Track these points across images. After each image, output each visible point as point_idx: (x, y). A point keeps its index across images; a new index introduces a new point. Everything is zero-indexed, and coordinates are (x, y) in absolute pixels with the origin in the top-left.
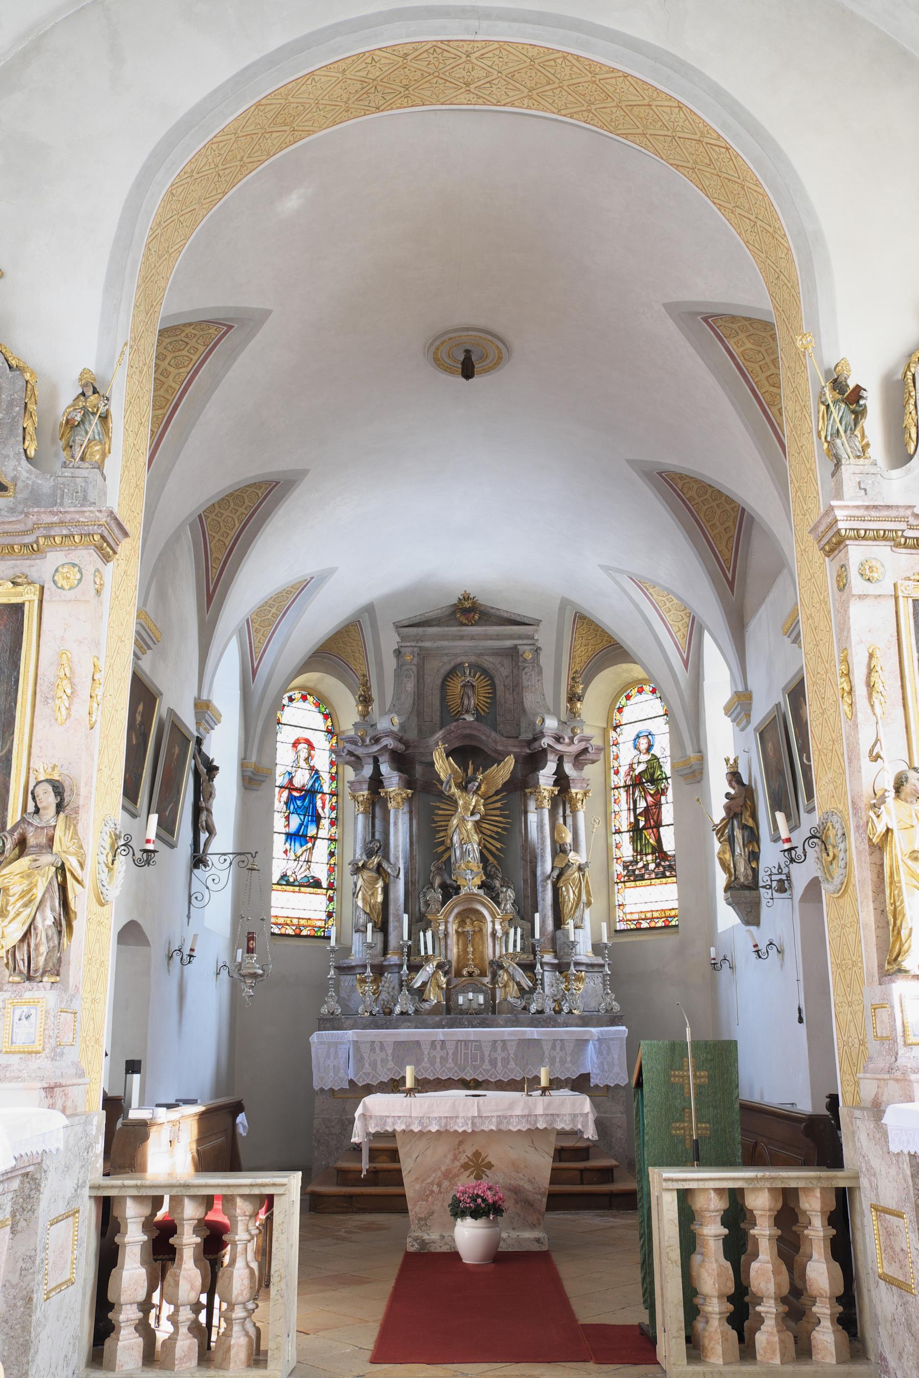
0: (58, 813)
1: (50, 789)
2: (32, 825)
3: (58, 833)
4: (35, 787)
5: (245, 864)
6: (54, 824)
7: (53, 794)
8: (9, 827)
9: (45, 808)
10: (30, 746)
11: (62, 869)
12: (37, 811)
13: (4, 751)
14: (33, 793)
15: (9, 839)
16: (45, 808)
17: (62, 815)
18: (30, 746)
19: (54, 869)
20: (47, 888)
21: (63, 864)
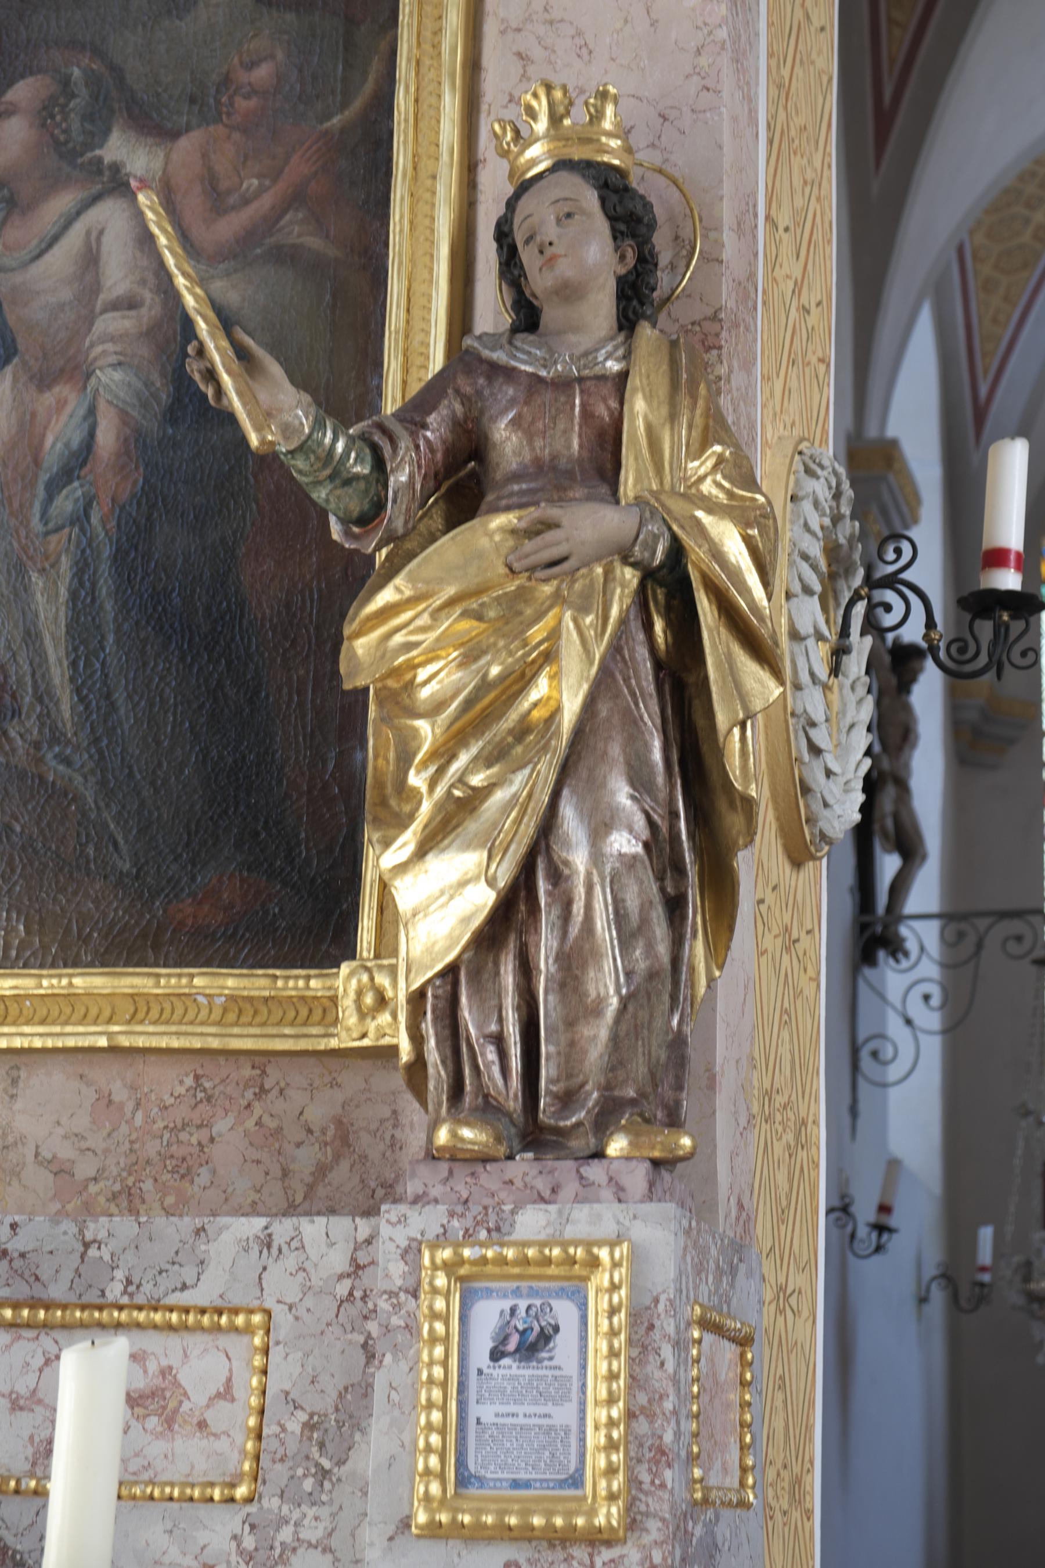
0: (627, 321)
1: (590, 198)
2: (509, 373)
3: (639, 409)
4: (511, 204)
5: (1027, 943)
6: (613, 366)
7: (602, 225)
8: (391, 404)
9: (570, 292)
10: (473, 66)
11: (671, 585)
12: (527, 317)
13: (357, 104)
14: (503, 234)
15: (404, 443)
16: (570, 292)
17: (646, 332)
18: (473, 66)
19: (630, 576)
20: (605, 671)
21: (677, 551)
